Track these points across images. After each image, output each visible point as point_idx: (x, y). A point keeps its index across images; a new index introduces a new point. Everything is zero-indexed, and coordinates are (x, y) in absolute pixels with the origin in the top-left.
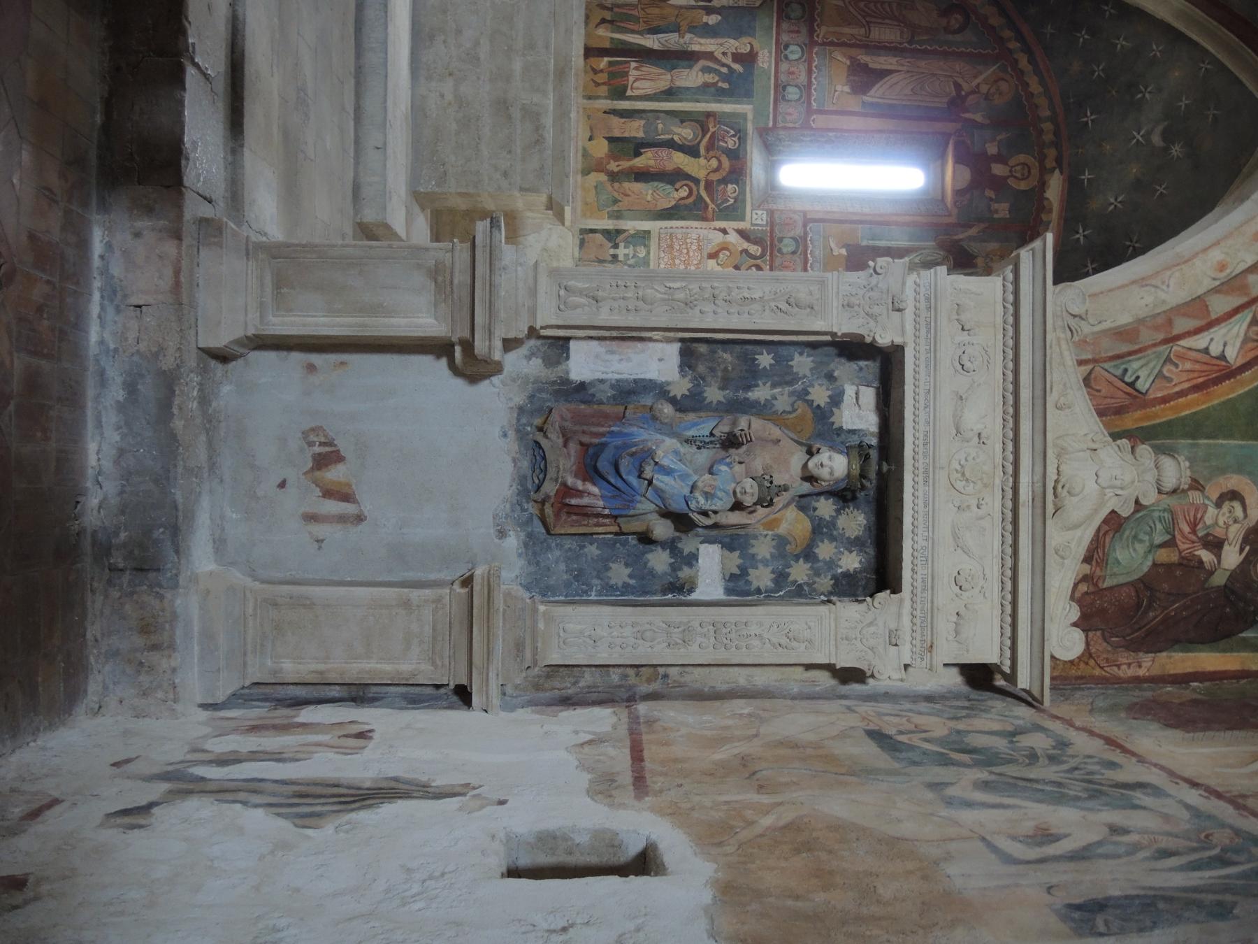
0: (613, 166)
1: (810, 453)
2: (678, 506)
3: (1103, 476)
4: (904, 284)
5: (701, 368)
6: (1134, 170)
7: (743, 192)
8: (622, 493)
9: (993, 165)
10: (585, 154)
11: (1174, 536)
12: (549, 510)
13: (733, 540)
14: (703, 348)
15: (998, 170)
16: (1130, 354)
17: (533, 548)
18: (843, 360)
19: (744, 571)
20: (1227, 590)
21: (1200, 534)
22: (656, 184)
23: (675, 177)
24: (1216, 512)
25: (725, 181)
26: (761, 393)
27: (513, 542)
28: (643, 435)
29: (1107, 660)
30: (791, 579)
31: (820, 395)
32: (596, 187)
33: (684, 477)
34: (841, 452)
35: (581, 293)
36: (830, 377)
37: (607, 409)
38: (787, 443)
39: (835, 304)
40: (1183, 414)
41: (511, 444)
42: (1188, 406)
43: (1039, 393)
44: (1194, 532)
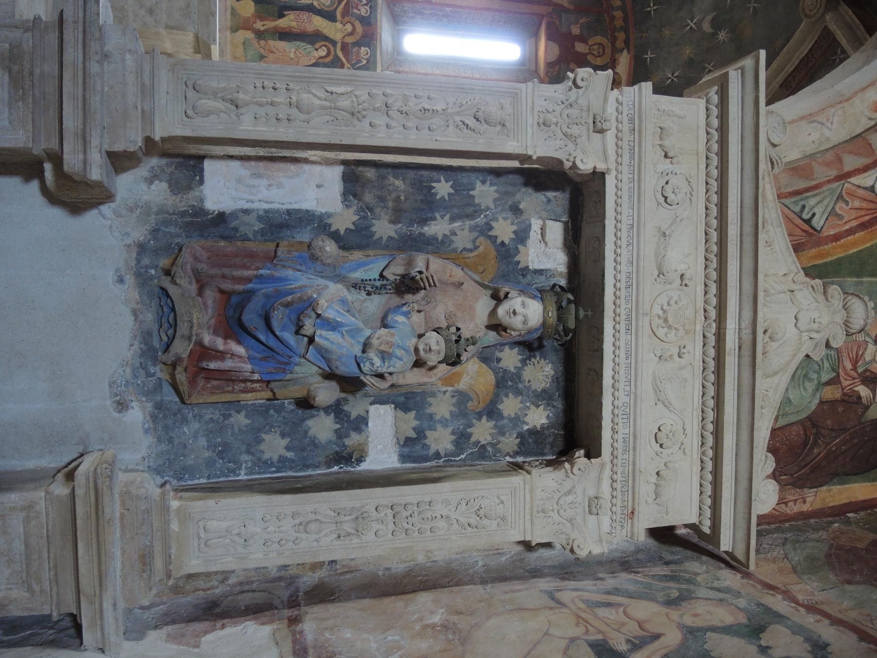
0: (259, 25)
1: (498, 298)
2: (348, 369)
3: (800, 319)
4: (605, 100)
5: (369, 197)
6: (688, 51)
7: (374, 54)
8: (277, 358)
9: (576, 43)
10: (234, 12)
11: (838, 374)
12: (181, 377)
13: (406, 401)
14: (370, 173)
15: (580, 47)
16: (808, 190)
17: (162, 421)
18: (530, 190)
19: (421, 434)
21: (860, 370)
22: (298, 43)
23: (315, 38)
25: (358, 44)
26: (437, 228)
27: (137, 414)
28: (301, 280)
30: (473, 439)
31: (504, 230)
32: (244, 43)
33: (354, 332)
34: (534, 297)
35: (215, 95)
36: (516, 210)
37: (250, 245)
38: (470, 286)
39: (530, 121)
40: (851, 252)
41: (130, 291)
42: (855, 244)
43: (748, 229)
44: (855, 369)
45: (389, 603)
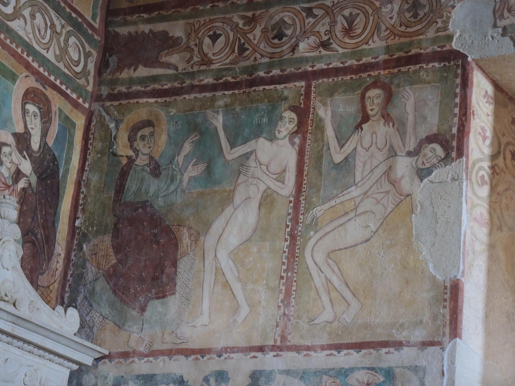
20: (41, 179)
24: (4, 167)
29: (52, 276)
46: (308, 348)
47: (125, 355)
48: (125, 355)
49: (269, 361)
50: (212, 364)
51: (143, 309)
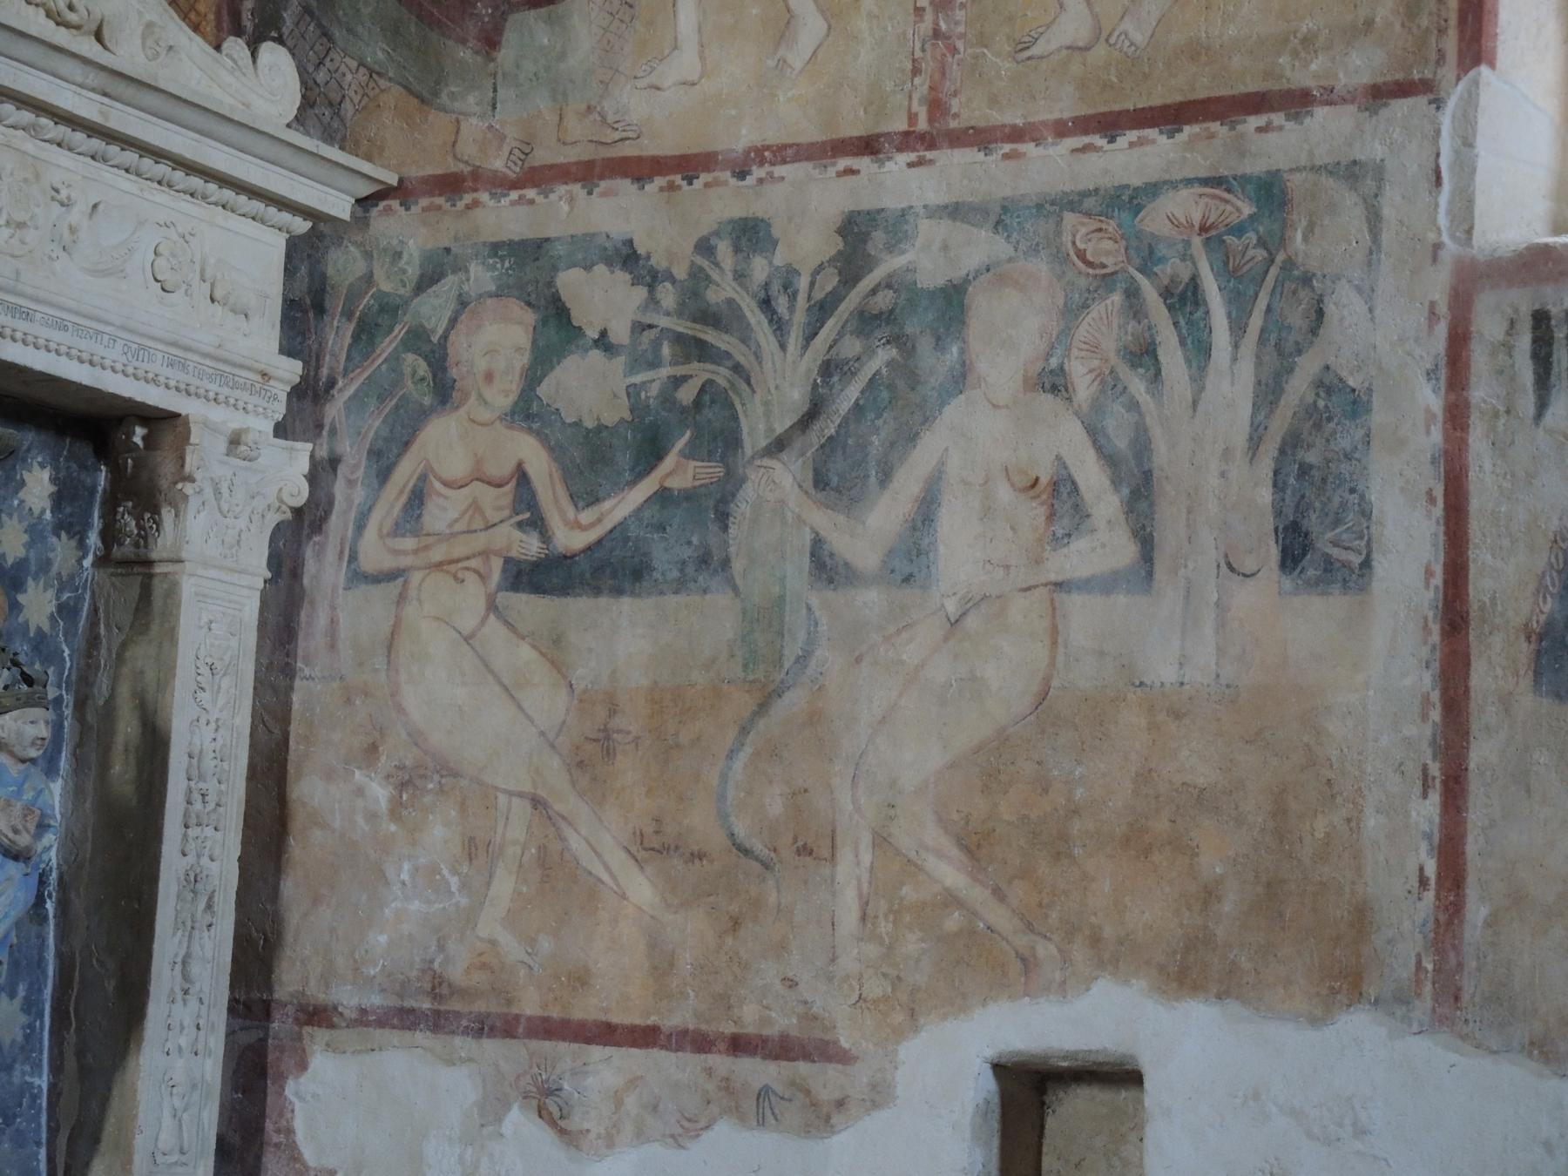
30: (46, 627)
45: (307, 848)
46: (1016, 135)
47: (450, 185)
48: (450, 185)
49: (896, 182)
50: (723, 201)
51: (491, 42)
